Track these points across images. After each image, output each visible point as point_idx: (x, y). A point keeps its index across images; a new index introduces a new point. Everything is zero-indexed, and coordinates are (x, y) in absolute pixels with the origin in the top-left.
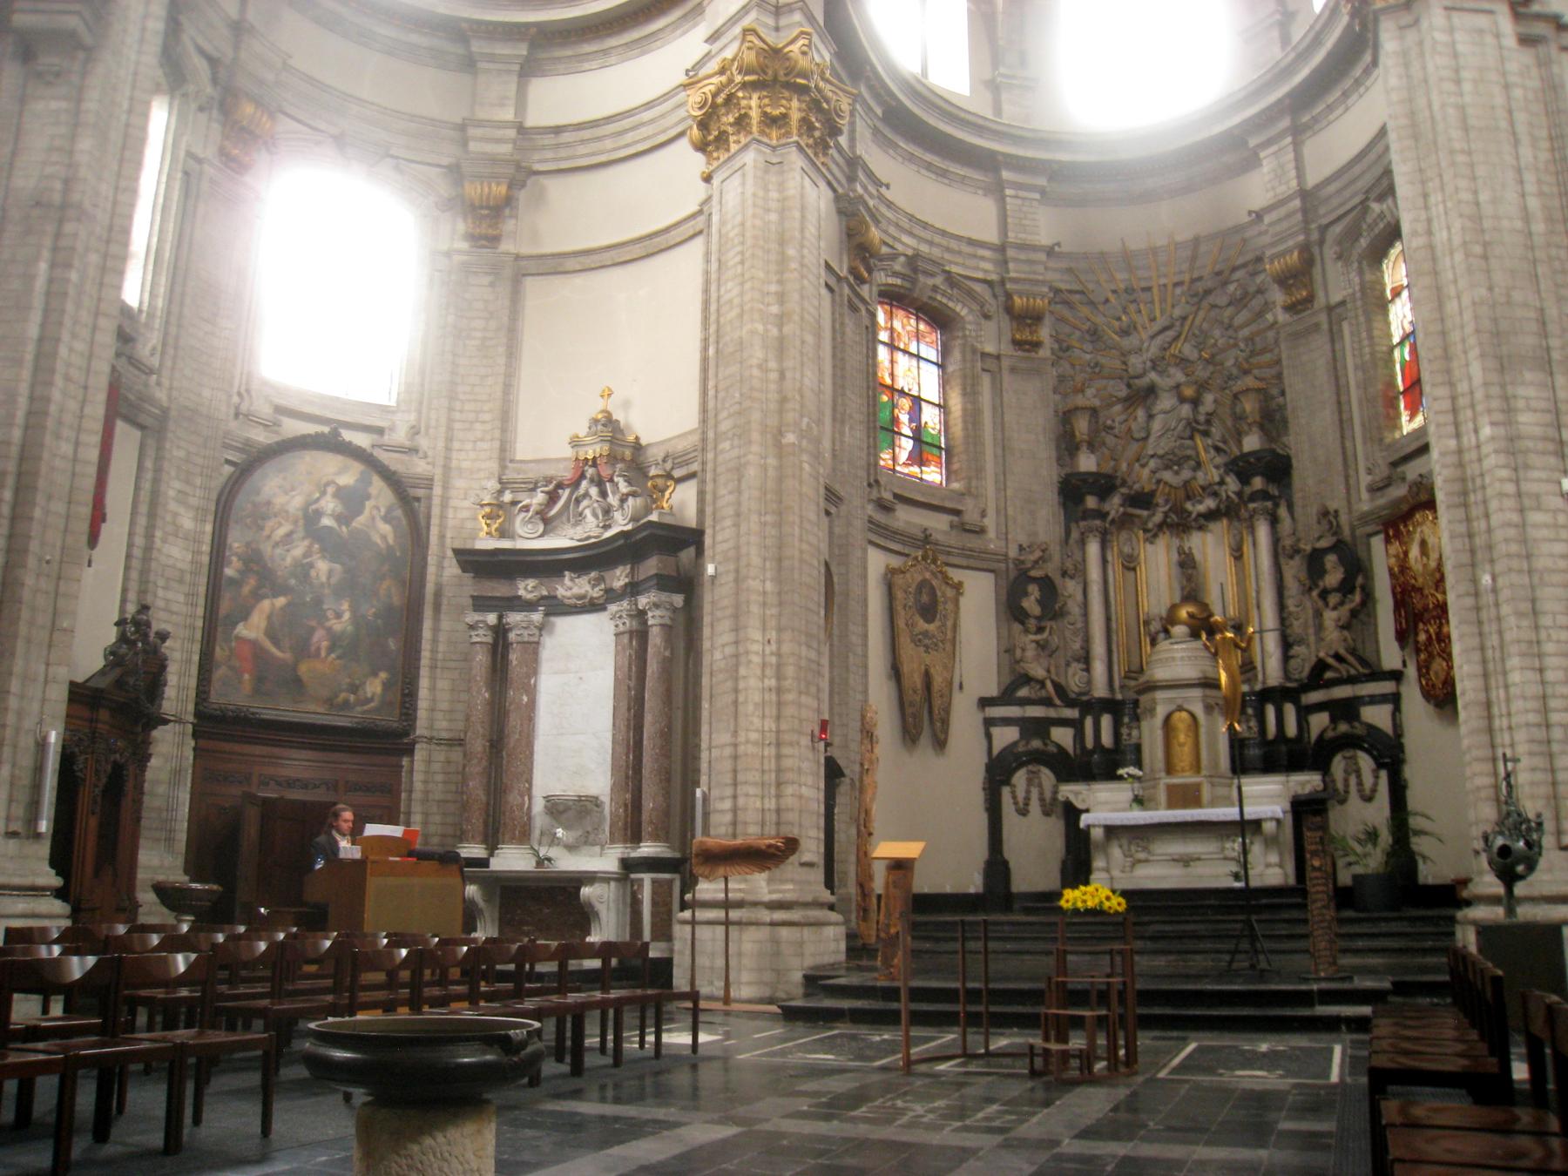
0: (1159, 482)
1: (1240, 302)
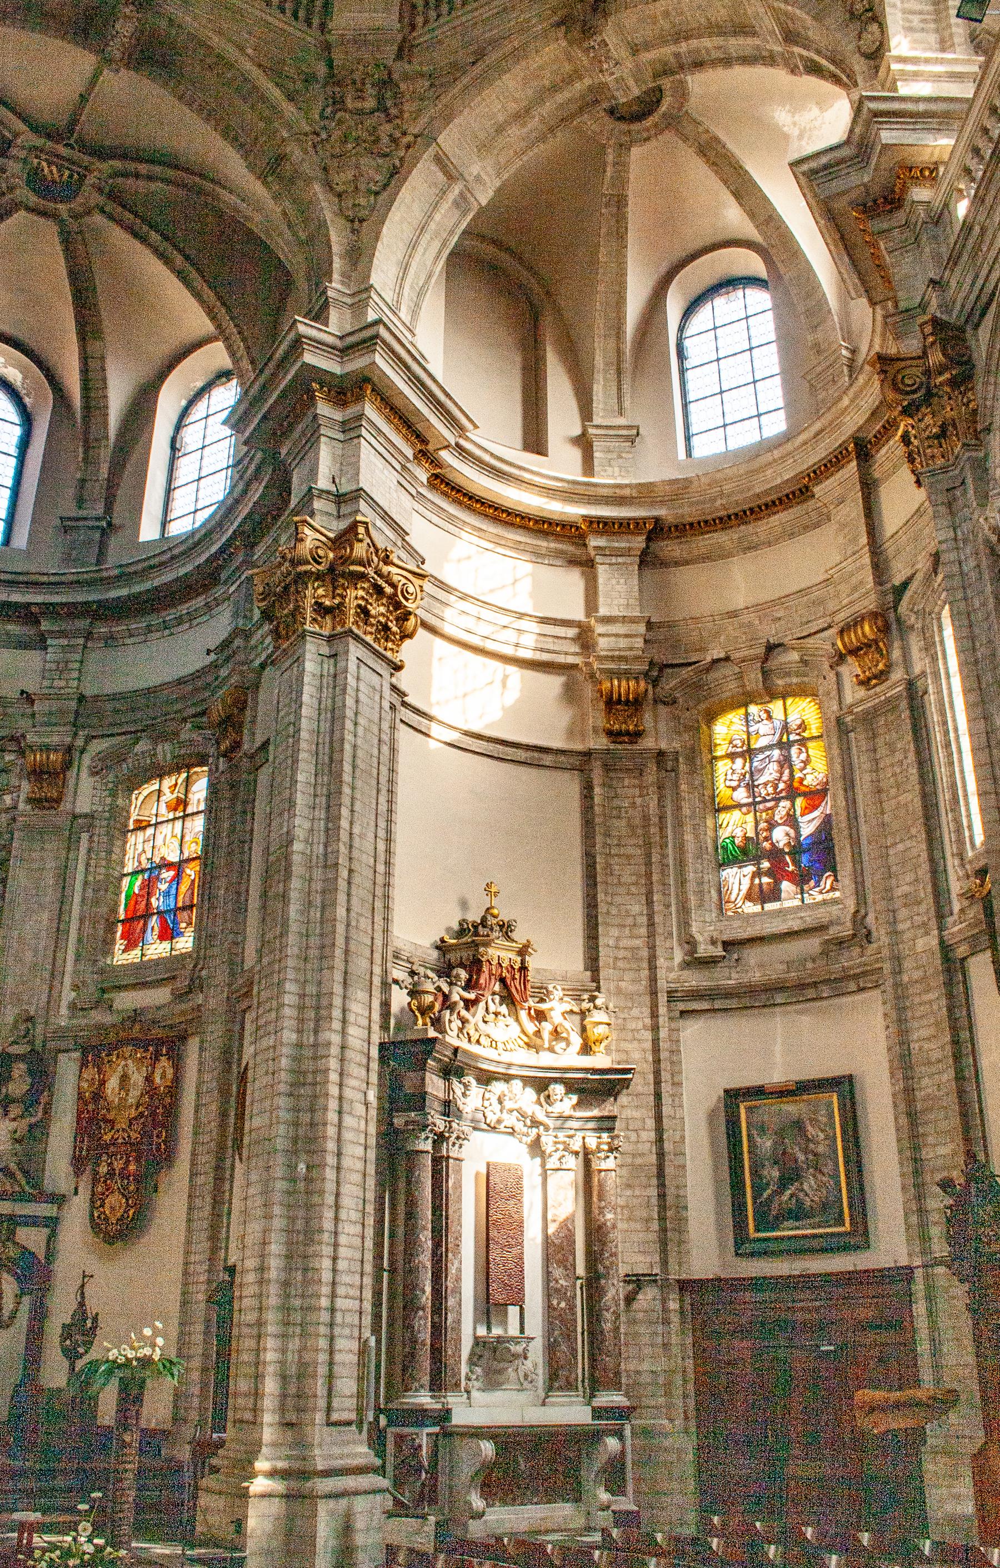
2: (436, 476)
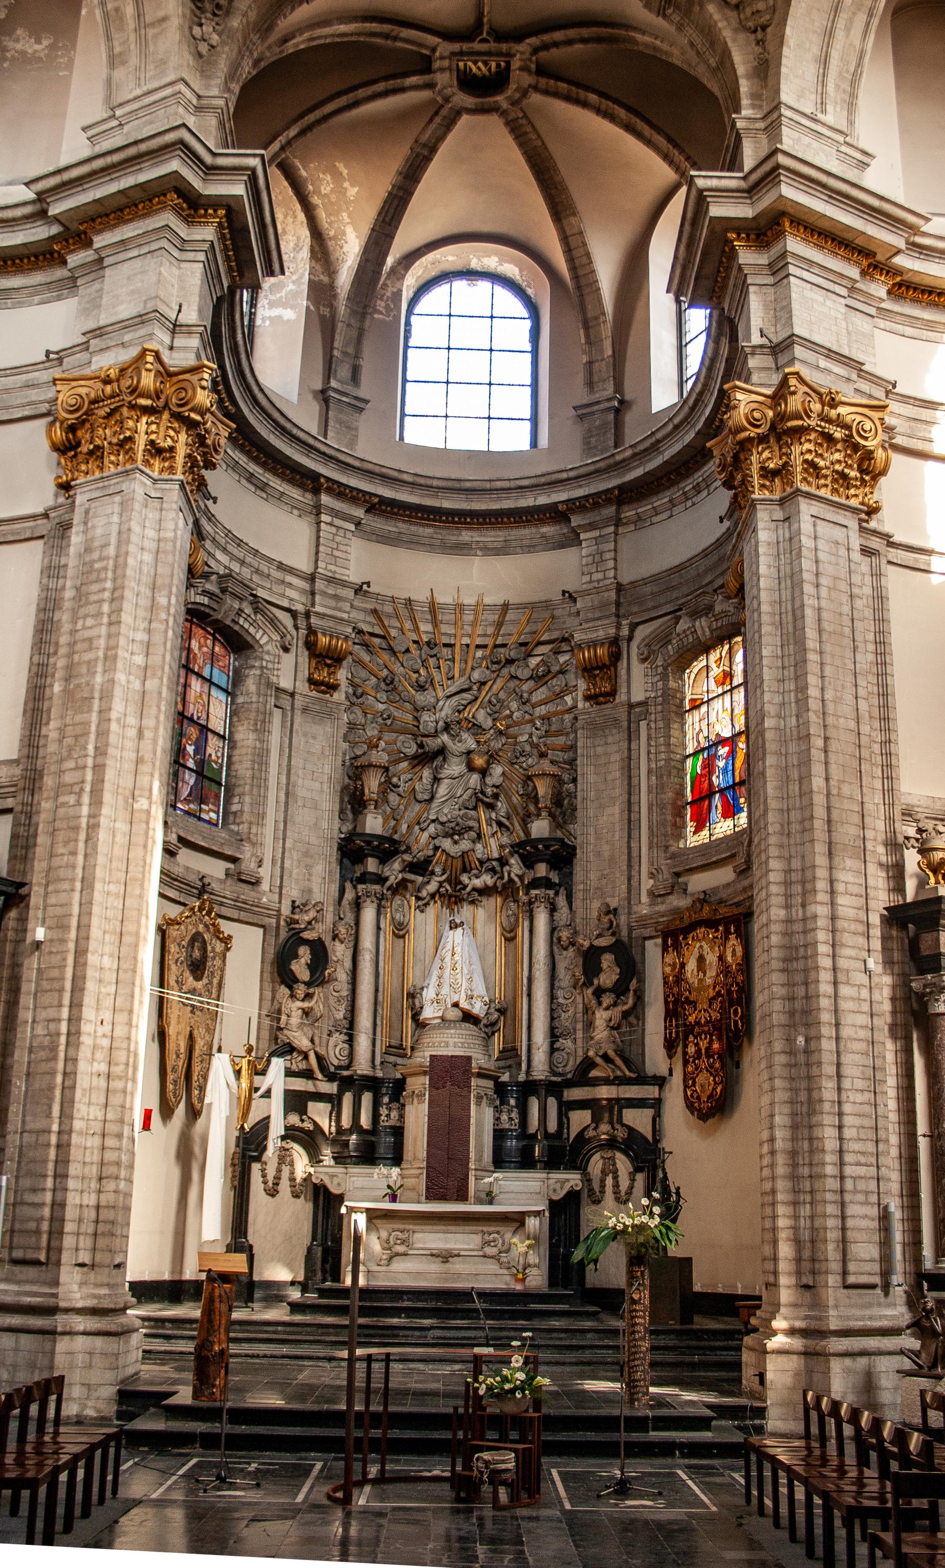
0: (436, 848)
1: (540, 678)
2: (900, 285)
